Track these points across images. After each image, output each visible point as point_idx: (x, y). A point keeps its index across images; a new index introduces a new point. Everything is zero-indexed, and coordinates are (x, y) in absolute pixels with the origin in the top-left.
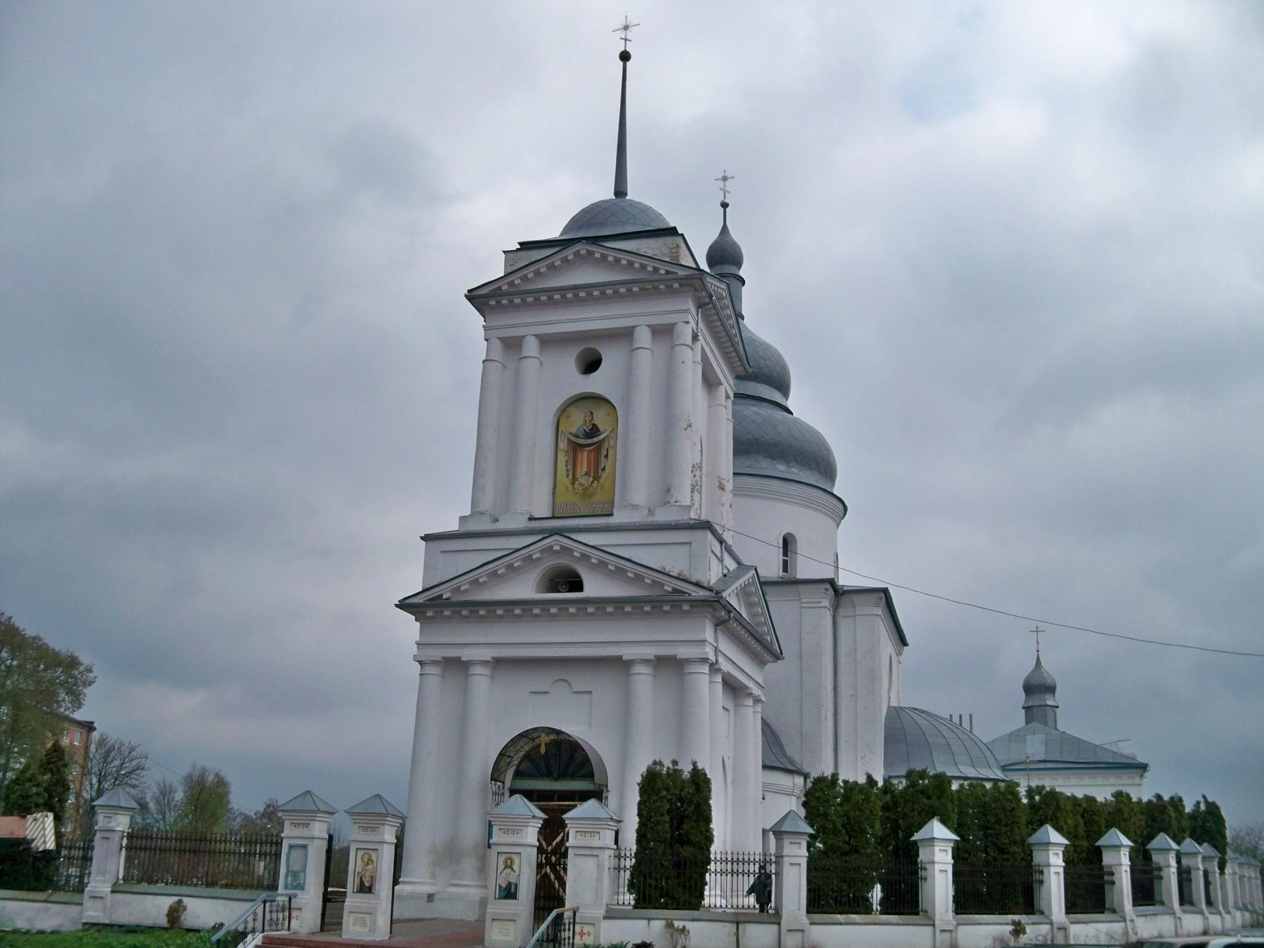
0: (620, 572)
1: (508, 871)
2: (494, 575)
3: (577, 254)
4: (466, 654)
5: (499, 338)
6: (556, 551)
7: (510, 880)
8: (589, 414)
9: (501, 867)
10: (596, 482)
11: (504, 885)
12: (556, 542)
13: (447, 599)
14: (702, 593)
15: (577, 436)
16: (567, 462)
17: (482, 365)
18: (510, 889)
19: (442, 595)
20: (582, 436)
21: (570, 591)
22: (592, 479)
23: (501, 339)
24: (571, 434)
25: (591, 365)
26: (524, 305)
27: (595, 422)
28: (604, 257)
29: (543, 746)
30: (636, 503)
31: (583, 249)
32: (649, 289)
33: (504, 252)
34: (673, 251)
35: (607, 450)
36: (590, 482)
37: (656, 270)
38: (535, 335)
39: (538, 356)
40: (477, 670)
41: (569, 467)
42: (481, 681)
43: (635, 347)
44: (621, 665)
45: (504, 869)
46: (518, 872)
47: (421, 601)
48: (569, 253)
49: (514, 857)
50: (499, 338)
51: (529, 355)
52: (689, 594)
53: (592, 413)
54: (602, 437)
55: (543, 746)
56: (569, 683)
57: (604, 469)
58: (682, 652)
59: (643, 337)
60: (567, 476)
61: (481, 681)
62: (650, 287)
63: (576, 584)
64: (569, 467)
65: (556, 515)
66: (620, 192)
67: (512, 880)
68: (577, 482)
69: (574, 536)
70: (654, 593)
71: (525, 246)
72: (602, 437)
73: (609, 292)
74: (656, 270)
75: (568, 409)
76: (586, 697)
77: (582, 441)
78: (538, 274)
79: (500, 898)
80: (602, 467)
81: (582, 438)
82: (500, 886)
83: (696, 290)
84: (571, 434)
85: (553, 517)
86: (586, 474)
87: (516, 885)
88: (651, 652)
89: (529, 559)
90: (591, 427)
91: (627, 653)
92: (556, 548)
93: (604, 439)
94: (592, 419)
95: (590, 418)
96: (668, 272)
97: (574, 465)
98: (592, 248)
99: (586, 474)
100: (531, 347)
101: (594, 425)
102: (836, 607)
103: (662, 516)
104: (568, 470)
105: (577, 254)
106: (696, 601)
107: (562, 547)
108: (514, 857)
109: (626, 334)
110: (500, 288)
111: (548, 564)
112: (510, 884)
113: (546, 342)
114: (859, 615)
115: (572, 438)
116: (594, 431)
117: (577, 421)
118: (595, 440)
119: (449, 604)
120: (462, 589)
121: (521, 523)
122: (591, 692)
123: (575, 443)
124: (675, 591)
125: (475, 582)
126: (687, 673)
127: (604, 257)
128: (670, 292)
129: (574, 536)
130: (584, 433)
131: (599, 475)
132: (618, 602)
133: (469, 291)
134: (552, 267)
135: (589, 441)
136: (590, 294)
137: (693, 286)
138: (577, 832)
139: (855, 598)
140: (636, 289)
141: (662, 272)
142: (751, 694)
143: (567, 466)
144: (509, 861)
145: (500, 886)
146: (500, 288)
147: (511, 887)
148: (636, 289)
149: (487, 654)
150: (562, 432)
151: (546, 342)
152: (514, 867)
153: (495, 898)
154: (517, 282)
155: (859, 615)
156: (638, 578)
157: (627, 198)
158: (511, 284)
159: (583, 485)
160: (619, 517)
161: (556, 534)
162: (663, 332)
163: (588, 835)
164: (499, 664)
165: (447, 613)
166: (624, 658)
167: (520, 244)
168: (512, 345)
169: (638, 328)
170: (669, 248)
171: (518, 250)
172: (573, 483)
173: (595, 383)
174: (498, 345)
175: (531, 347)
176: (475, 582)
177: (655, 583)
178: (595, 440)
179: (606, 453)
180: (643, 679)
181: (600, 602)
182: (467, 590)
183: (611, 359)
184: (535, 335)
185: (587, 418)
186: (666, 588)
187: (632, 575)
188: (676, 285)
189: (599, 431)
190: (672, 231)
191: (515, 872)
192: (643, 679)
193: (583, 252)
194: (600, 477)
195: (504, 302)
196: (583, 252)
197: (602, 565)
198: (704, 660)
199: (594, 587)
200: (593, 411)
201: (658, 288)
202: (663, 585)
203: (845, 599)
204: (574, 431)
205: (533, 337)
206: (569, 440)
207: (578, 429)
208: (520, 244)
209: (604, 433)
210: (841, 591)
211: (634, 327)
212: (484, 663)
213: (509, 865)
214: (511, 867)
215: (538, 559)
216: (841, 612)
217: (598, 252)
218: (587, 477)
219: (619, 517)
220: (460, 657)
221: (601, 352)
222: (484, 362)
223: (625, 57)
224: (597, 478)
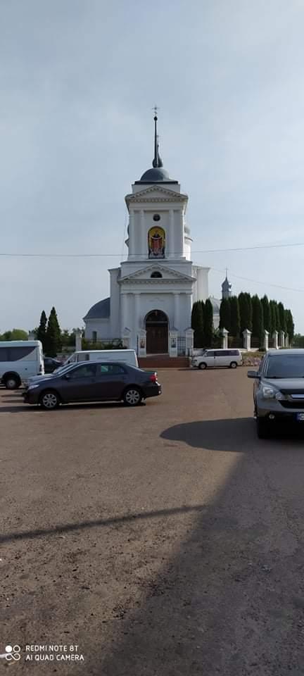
4: (134, 292)
25: (157, 218)
42: (138, 299)
58: (187, 292)
59: (172, 212)
61: (138, 299)
63: (160, 276)
88: (179, 292)
89: (149, 270)
91: (174, 292)
109: (167, 211)
151: (145, 211)
168: (136, 212)
180: (177, 298)
192: (177, 298)
197: (167, 271)
199: (165, 276)
223: (156, 119)
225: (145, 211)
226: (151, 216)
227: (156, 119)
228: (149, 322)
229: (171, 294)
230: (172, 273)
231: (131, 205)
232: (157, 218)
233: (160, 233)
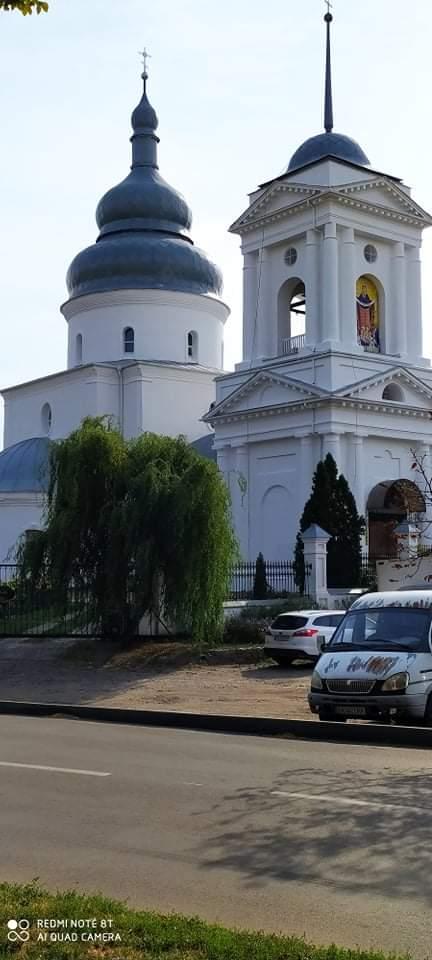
4: (234, 443)
25: (292, 257)
37: (311, 191)
40: (239, 451)
44: (299, 439)
58: (321, 430)
66: (328, 125)
69: (273, 371)
71: (262, 186)
85: (283, 356)
88: (306, 432)
91: (298, 433)
100: (263, 255)
109: (302, 237)
129: (273, 371)
133: (231, 227)
142: (425, 445)
157: (334, 131)
162: (320, 231)
164: (250, 445)
175: (263, 255)
177: (306, 392)
198: (332, 434)
212: (241, 447)
225: (271, 248)
226: (280, 255)
227: (328, 18)
229: (293, 437)
230: (290, 386)
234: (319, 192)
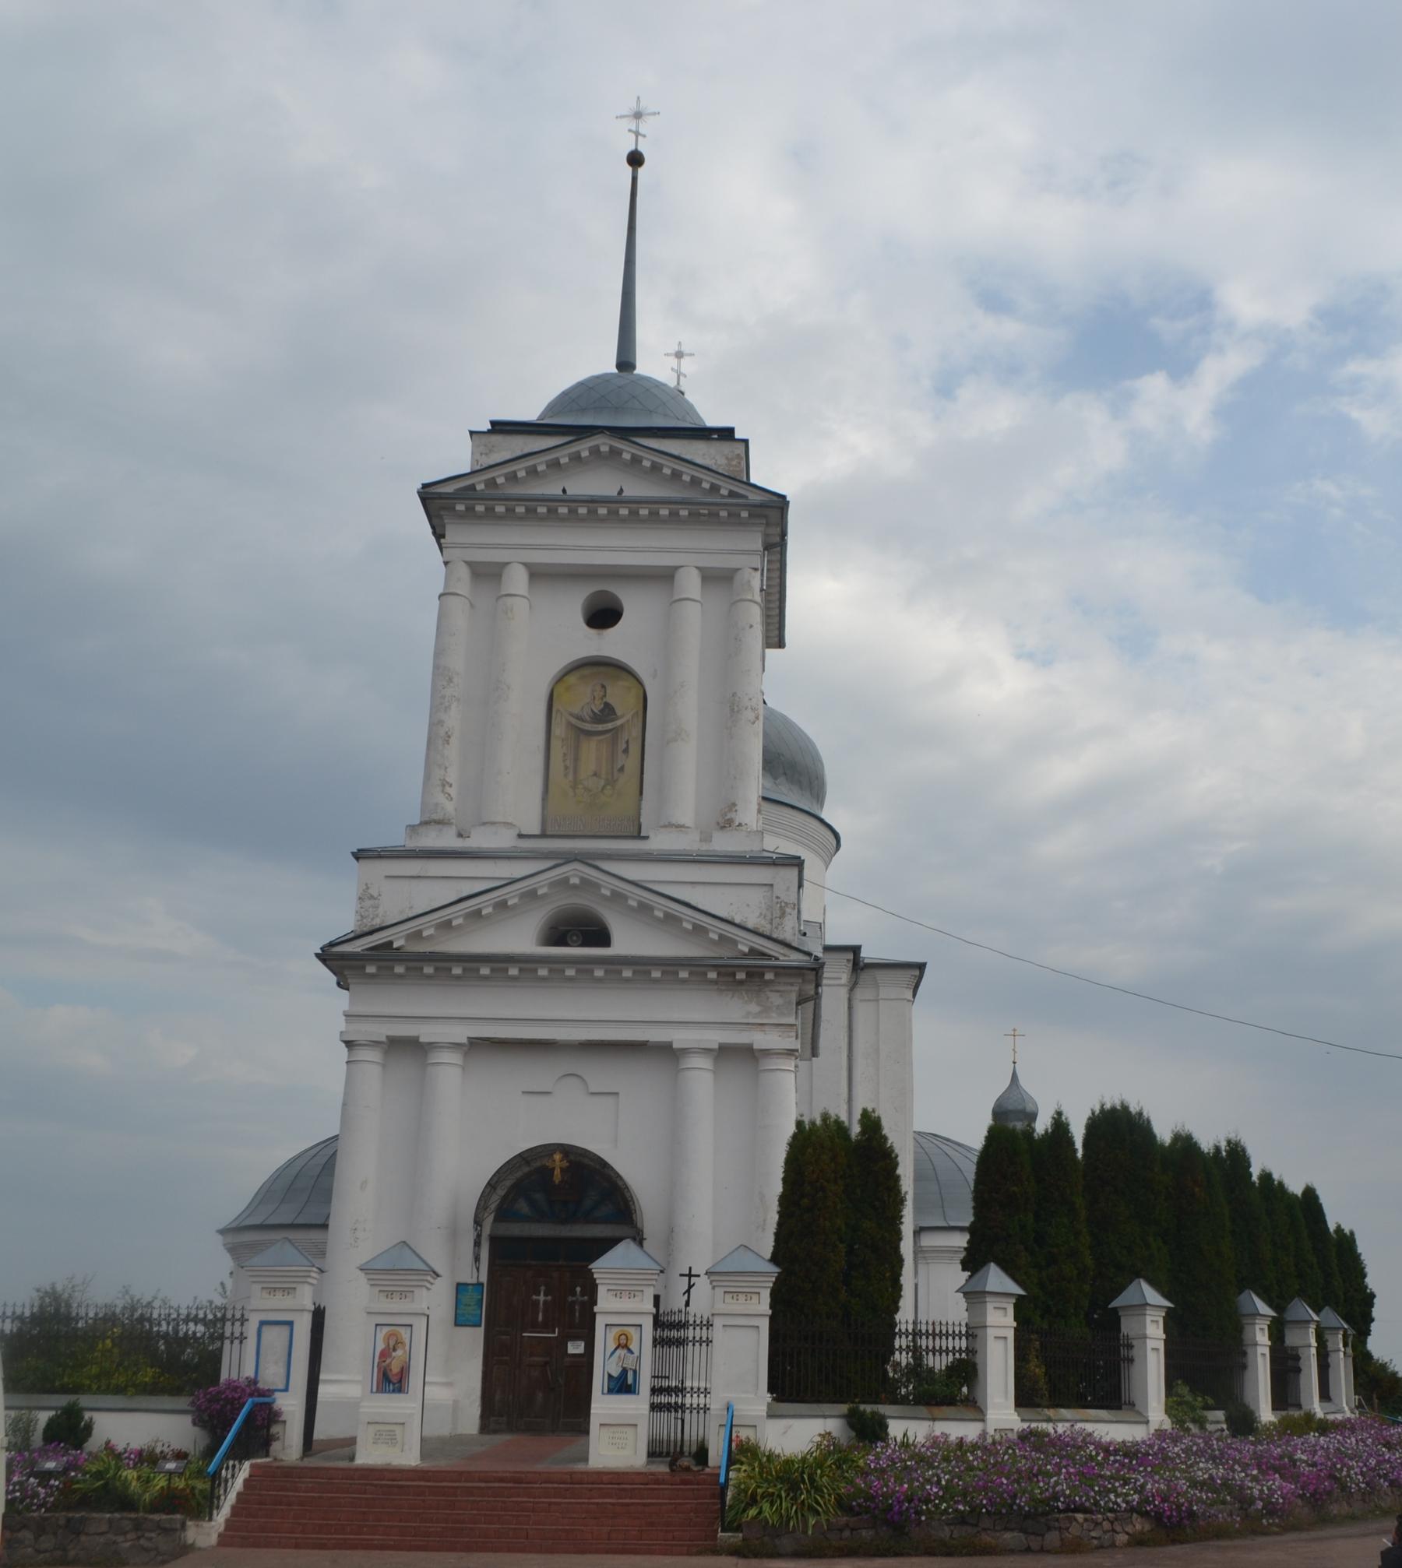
0: (670, 919)
1: (621, 1352)
2: (477, 914)
3: (595, 451)
4: (427, 1033)
5: (466, 562)
6: (575, 887)
7: (625, 1366)
8: (598, 688)
9: (612, 1346)
10: (609, 787)
11: (615, 1373)
12: (574, 872)
13: (397, 949)
14: (795, 959)
15: (580, 718)
16: (565, 755)
17: (438, 602)
18: (626, 1378)
19: (391, 943)
20: (588, 719)
21: (583, 945)
22: (602, 783)
23: (469, 564)
24: (571, 715)
25: (603, 616)
26: (510, 516)
27: (608, 699)
28: (636, 460)
29: (557, 1172)
30: (681, 822)
31: (604, 444)
32: (704, 515)
33: (472, 433)
34: (734, 463)
35: (627, 742)
36: (600, 789)
38: (525, 564)
39: (526, 594)
40: (446, 1057)
41: (568, 763)
43: (676, 597)
44: (667, 1053)
45: (616, 1349)
46: (637, 1353)
47: (359, 950)
48: (584, 447)
49: (632, 1331)
50: (466, 562)
51: (513, 592)
52: (777, 959)
53: (603, 686)
54: (618, 723)
55: (557, 1172)
56: (583, 1080)
57: (622, 769)
59: (690, 583)
60: (566, 775)
62: (706, 512)
64: (568, 763)
65: (549, 833)
67: (630, 1363)
68: (580, 786)
69: (599, 863)
70: (724, 952)
71: (500, 428)
72: (618, 723)
73: (644, 512)
74: (715, 489)
75: (566, 678)
76: (611, 1100)
77: (588, 727)
78: (532, 472)
79: (610, 1391)
80: (619, 767)
81: (587, 722)
82: (610, 1376)
83: (768, 524)
84: (571, 715)
85: (543, 835)
86: (595, 774)
87: (635, 1372)
88: (715, 1038)
89: (531, 895)
90: (602, 706)
91: (679, 1038)
92: (575, 881)
93: (622, 726)
94: (605, 696)
95: (602, 693)
96: (732, 494)
97: (576, 759)
98: (619, 444)
99: (595, 774)
100: (517, 580)
101: (607, 705)
102: (853, 987)
103: (724, 843)
104: (566, 768)
105: (595, 451)
106: (784, 968)
107: (583, 880)
108: (632, 1331)
109: (665, 577)
110: (472, 487)
111: (559, 904)
112: (625, 1371)
113: (538, 574)
114: (882, 999)
115: (574, 721)
116: (607, 712)
117: (582, 698)
118: (609, 726)
119: (400, 956)
120: (425, 934)
121: (504, 840)
122: (617, 1094)
123: (576, 727)
124: (754, 952)
125: (447, 925)
126: (761, 1071)
127: (636, 460)
128: (733, 521)
130: (592, 715)
131: (615, 778)
132: (670, 966)
134: (555, 465)
135: (600, 727)
136: (592, 512)
137: (766, 517)
138: (725, 1292)
139: (881, 975)
140: (684, 513)
141: (724, 492)
143: (564, 761)
144: (623, 1337)
145: (610, 1376)
146: (472, 487)
147: (627, 1374)
148: (684, 513)
149: (461, 1033)
150: (558, 711)
151: (538, 574)
152: (631, 1347)
153: (603, 1393)
154: (500, 480)
155: (882, 999)
156: (699, 930)
157: (635, 372)
158: (491, 483)
159: (590, 791)
160: (659, 841)
161: (576, 860)
163: (742, 1297)
164: (479, 1046)
165: (399, 969)
166: (675, 1046)
167: (493, 423)
168: (487, 574)
169: (681, 570)
170: (727, 458)
171: (489, 432)
172: (574, 786)
173: (610, 643)
174: (464, 572)
175: (517, 580)
176: (447, 925)
177: (723, 939)
178: (609, 726)
179: (624, 746)
180: (700, 1077)
181: (642, 966)
182: (430, 937)
183: (636, 605)
184: (525, 564)
185: (595, 694)
186: (740, 947)
187: (690, 927)
188: (744, 514)
189: (615, 714)
190: (727, 433)
191: (632, 1353)
192: (700, 1077)
193: (604, 449)
194: (617, 779)
195: (480, 508)
196: (604, 449)
197: (644, 909)
200: (604, 683)
201: (717, 515)
202: (735, 943)
203: (865, 976)
204: (576, 711)
205: (521, 566)
206: (570, 725)
207: (583, 708)
208: (493, 423)
209: (622, 716)
210: (861, 964)
211: (677, 568)
213: (623, 1345)
214: (626, 1347)
215: (544, 896)
216: (859, 993)
217: (627, 451)
218: (595, 778)
219: (659, 841)
220: (418, 1037)
221: (623, 601)
222: (440, 596)
224: (611, 782)
226: (572, 605)
228: (516, 1229)
231: (453, 534)
232: (603, 616)
233: (620, 696)
234: (745, 497)
